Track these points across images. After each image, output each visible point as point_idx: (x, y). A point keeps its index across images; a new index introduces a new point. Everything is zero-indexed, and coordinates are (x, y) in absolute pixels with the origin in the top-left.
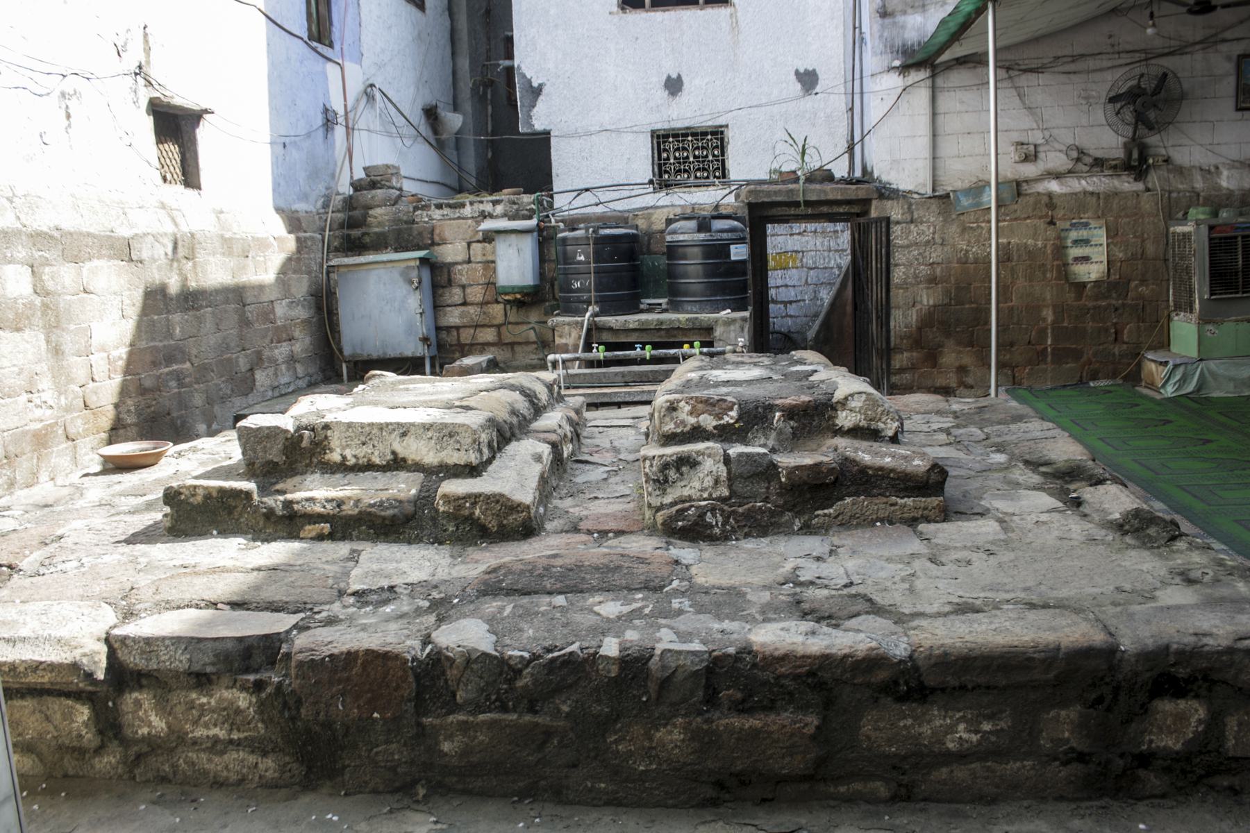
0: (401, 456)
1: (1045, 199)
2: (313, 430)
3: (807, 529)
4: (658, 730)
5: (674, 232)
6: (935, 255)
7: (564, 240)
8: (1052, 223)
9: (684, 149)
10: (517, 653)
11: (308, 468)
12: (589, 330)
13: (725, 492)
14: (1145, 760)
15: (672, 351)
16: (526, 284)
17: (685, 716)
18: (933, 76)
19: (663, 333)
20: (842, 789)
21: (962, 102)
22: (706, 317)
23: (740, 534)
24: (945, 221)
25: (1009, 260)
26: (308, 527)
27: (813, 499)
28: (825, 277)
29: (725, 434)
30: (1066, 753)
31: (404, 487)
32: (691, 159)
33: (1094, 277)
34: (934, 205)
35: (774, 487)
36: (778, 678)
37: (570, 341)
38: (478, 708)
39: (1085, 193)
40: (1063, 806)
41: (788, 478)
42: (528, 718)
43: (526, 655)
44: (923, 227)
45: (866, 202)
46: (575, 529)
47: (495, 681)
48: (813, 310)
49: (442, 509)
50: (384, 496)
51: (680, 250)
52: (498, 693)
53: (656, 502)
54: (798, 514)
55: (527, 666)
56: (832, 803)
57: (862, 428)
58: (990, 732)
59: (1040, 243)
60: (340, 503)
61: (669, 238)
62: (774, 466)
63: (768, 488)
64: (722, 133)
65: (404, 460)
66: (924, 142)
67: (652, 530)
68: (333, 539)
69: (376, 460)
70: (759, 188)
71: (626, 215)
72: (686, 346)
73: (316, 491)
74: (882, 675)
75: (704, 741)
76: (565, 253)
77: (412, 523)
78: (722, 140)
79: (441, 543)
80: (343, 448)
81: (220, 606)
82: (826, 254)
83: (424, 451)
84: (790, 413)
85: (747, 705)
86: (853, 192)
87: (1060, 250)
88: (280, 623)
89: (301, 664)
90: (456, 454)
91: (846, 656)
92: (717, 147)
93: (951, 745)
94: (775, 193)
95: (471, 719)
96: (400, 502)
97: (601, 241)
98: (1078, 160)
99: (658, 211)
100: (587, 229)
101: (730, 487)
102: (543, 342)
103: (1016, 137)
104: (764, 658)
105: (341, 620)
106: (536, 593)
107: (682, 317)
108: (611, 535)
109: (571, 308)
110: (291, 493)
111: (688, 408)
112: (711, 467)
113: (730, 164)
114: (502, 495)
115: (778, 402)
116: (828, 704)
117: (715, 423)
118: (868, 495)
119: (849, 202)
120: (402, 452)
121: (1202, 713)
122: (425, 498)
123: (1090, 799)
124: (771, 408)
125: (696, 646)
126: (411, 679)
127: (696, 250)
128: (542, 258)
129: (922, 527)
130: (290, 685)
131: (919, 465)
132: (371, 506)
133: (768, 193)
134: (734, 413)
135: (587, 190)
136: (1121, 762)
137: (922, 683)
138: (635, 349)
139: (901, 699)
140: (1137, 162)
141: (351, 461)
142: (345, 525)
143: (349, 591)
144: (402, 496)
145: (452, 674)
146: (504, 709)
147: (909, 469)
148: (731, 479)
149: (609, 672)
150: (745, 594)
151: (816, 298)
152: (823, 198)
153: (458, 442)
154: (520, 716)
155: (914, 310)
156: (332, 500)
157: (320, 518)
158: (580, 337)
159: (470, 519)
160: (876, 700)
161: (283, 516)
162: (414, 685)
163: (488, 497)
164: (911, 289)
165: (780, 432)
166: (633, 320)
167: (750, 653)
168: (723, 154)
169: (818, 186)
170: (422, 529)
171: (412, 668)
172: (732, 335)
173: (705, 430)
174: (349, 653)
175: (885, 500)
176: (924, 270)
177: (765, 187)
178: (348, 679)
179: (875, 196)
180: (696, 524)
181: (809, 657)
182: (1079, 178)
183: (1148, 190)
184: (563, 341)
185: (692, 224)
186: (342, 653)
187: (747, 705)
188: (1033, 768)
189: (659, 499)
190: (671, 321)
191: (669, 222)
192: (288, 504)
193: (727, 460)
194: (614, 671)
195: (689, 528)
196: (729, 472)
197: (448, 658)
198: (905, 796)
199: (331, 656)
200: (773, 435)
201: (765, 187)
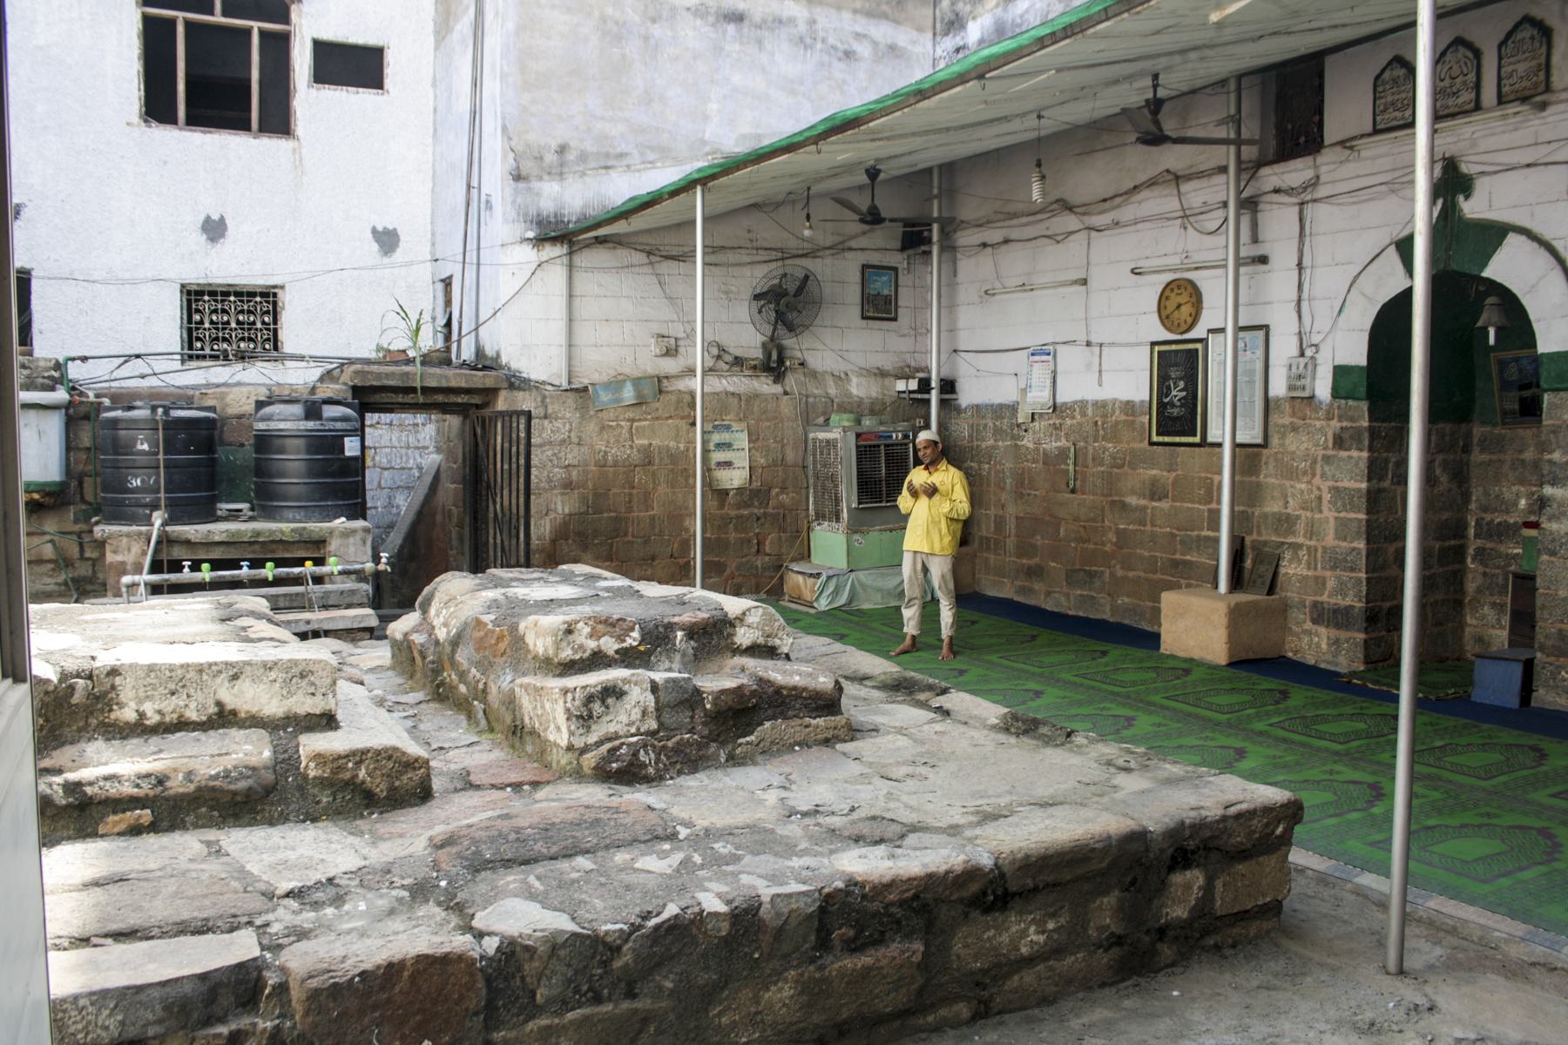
0: (229, 707)
2: (90, 677)
3: (734, 760)
4: (768, 989)
5: (269, 418)
6: (572, 456)
7: (115, 423)
10: (610, 927)
11: (85, 733)
12: (158, 543)
13: (654, 725)
14: (1162, 932)
15: (296, 570)
17: (798, 966)
18: (570, 254)
19: (257, 547)
20: (930, 1019)
22: (316, 527)
23: (673, 772)
24: (582, 417)
26: (112, 818)
27: (732, 725)
28: (401, 478)
29: (627, 657)
30: (1107, 939)
31: (249, 751)
33: (736, 484)
34: (571, 400)
35: (699, 714)
36: (886, 907)
37: (129, 558)
38: (565, 1005)
39: (727, 393)
40: (1107, 991)
41: (714, 704)
42: (626, 1005)
43: (625, 927)
44: (559, 424)
45: (492, 392)
46: (471, 786)
47: (586, 967)
48: (387, 520)
49: (312, 774)
50: (228, 762)
51: (278, 442)
52: (590, 981)
53: (579, 742)
54: (723, 744)
55: (626, 941)
56: (923, 1036)
57: (759, 646)
58: (1053, 931)
59: (682, 446)
60: (161, 780)
61: (261, 426)
62: (697, 692)
63: (692, 717)
65: (234, 713)
66: (558, 328)
67: (578, 775)
68: (157, 832)
69: (192, 715)
70: (366, 368)
71: (191, 392)
72: (309, 563)
73: (108, 765)
74: (974, 888)
75: (813, 992)
76: (115, 440)
77: (274, 797)
79: (314, 820)
80: (140, 701)
81: (95, 940)
82: (403, 451)
83: (264, 698)
84: (693, 632)
85: (859, 943)
86: (480, 379)
88: (241, 947)
89: (315, 994)
90: (309, 700)
91: (947, 872)
93: (1024, 950)
95: (557, 1021)
96: (254, 769)
97: (173, 426)
98: (719, 357)
100: (154, 409)
101: (658, 718)
102: (65, 560)
103: (657, 328)
104: (874, 888)
105: (311, 931)
106: (536, 861)
107: (286, 527)
108: (526, 787)
109: (118, 512)
110: (71, 770)
111: (587, 630)
112: (639, 697)
113: (283, 335)
114: (396, 749)
115: (676, 619)
116: (929, 928)
117: (616, 646)
118: (785, 718)
119: (468, 391)
120: (230, 701)
121: (1201, 881)
122: (286, 762)
123: (1123, 980)
124: (670, 627)
125: (795, 887)
126: (481, 984)
128: (70, 446)
129: (838, 746)
130: (294, 1027)
131: (824, 682)
132: (216, 777)
133: (379, 376)
134: (636, 634)
135: (138, 356)
136: (1147, 939)
137: (1006, 889)
138: (241, 568)
139: (988, 910)
140: (774, 365)
141: (153, 719)
142: (167, 809)
143: (279, 892)
144: (254, 761)
145: (531, 968)
146: (598, 1000)
147: (819, 687)
148: (659, 709)
149: (719, 930)
150: (772, 831)
151: (390, 505)
152: (444, 384)
153: (313, 684)
154: (616, 1006)
155: (547, 519)
156: (148, 776)
157: (134, 802)
158: (144, 553)
159: (352, 785)
160: (966, 915)
161: (68, 806)
162: (484, 992)
163: (378, 752)
164: (544, 495)
165: (684, 655)
166: (218, 530)
167: (856, 884)
169: (437, 371)
170: (288, 805)
171: (481, 970)
172: (352, 549)
173: (606, 656)
174: (390, 965)
175: (799, 721)
176: (559, 473)
177: (375, 368)
178: (389, 1001)
179: (505, 385)
180: (631, 764)
181: (914, 879)
183: (786, 393)
184: (119, 558)
185: (297, 409)
186: (379, 967)
187: (859, 943)
188: (1084, 959)
189: (583, 739)
190: (272, 532)
191: (260, 405)
192: (73, 788)
193: (654, 688)
194: (725, 928)
195: (626, 773)
196: (657, 702)
197: (527, 948)
198: (984, 1012)
199: (363, 974)
200: (678, 657)
201: (375, 368)
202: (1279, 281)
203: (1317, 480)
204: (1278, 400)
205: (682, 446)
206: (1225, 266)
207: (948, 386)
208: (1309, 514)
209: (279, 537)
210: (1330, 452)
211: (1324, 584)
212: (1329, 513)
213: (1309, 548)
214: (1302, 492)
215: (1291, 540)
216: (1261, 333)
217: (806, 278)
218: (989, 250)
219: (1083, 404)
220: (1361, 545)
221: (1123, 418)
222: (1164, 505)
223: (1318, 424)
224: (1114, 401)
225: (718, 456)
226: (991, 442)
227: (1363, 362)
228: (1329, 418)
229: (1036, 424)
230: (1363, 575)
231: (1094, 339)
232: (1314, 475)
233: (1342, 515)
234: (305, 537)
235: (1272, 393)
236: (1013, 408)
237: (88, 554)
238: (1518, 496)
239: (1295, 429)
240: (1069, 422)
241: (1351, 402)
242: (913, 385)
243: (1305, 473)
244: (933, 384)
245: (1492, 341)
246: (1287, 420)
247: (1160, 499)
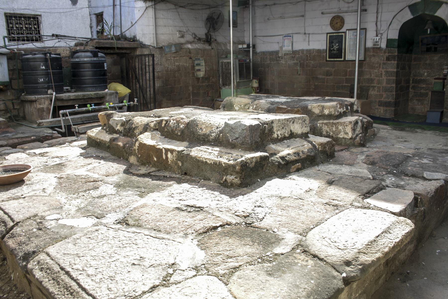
1: (188, 50)
8: (190, 58)
9: (20, 24)
16: (6, 81)
18: (155, 4)
19: (82, 100)
21: (163, 15)
24: (161, 56)
25: (180, 70)
32: (24, 29)
33: (202, 76)
45: (135, 49)
59: (187, 65)
64: (37, 18)
78: (38, 21)
86: (132, 45)
87: (193, 67)
92: (35, 24)
94: (106, 43)
98: (195, 38)
99: (59, 48)
103: (178, 29)
127: (89, 65)
133: (103, 43)
140: (208, 40)
152: (123, 46)
168: (38, 28)
179: (140, 46)
182: (196, 44)
183: (212, 49)
184: (42, 106)
190: (88, 95)
202: (371, 17)
203: (381, 69)
204: (369, 48)
205: (187, 65)
206: (357, 12)
207: (254, 46)
208: (378, 78)
209: (91, 96)
210: (385, 62)
211: (382, 96)
212: (384, 78)
213: (378, 87)
214: (376, 72)
215: (372, 85)
216: (365, 30)
217: (220, 13)
218: (268, 7)
219: (302, 51)
220: (394, 85)
221: (317, 54)
222: (331, 77)
223: (381, 54)
224: (314, 49)
225: (197, 68)
226: (269, 62)
227: (397, 38)
228: (385, 52)
229: (286, 57)
230: (394, 93)
231: (307, 32)
232: (380, 68)
234: (98, 96)
235: (367, 46)
236: (277, 52)
237: (16, 107)
238: (424, 72)
239: (374, 56)
240: (297, 56)
241: (392, 49)
242: (245, 46)
243: (377, 67)
244: (251, 46)
246: (372, 54)
247: (330, 76)
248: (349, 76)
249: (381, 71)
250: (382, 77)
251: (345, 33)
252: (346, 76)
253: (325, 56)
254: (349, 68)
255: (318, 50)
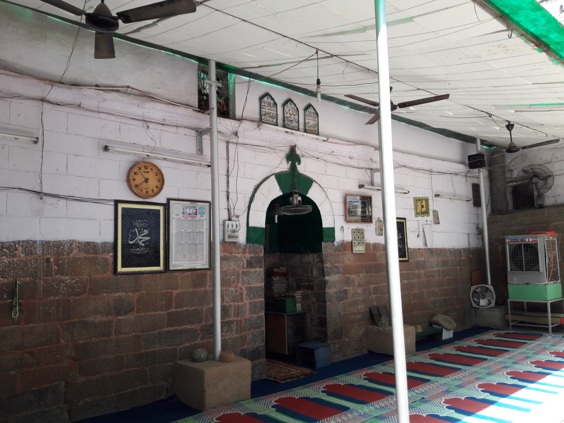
203: (240, 285)
208: (236, 304)
210: (245, 270)
213: (237, 322)
214: (232, 292)
222: (131, 316)
223: (239, 255)
224: (71, 242)
232: (238, 282)
233: (252, 301)
243: (234, 282)
245: (276, 222)
247: (126, 313)
248: (175, 307)
249: (241, 289)
250: (242, 301)
251: (167, 206)
252: (170, 308)
253: (111, 260)
254: (177, 289)
255: (88, 243)
